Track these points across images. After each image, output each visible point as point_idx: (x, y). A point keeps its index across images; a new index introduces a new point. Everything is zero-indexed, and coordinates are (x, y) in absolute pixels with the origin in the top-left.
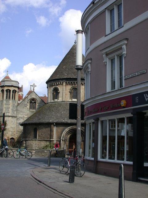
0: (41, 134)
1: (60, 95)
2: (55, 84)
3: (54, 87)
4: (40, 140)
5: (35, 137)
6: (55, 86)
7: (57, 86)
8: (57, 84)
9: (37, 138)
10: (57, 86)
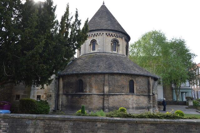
0: (140, 88)
1: (121, 47)
2: (116, 36)
3: (112, 38)
4: (138, 95)
5: (132, 91)
6: (114, 37)
7: (117, 39)
8: (118, 36)
9: (134, 92)
10: (117, 39)
